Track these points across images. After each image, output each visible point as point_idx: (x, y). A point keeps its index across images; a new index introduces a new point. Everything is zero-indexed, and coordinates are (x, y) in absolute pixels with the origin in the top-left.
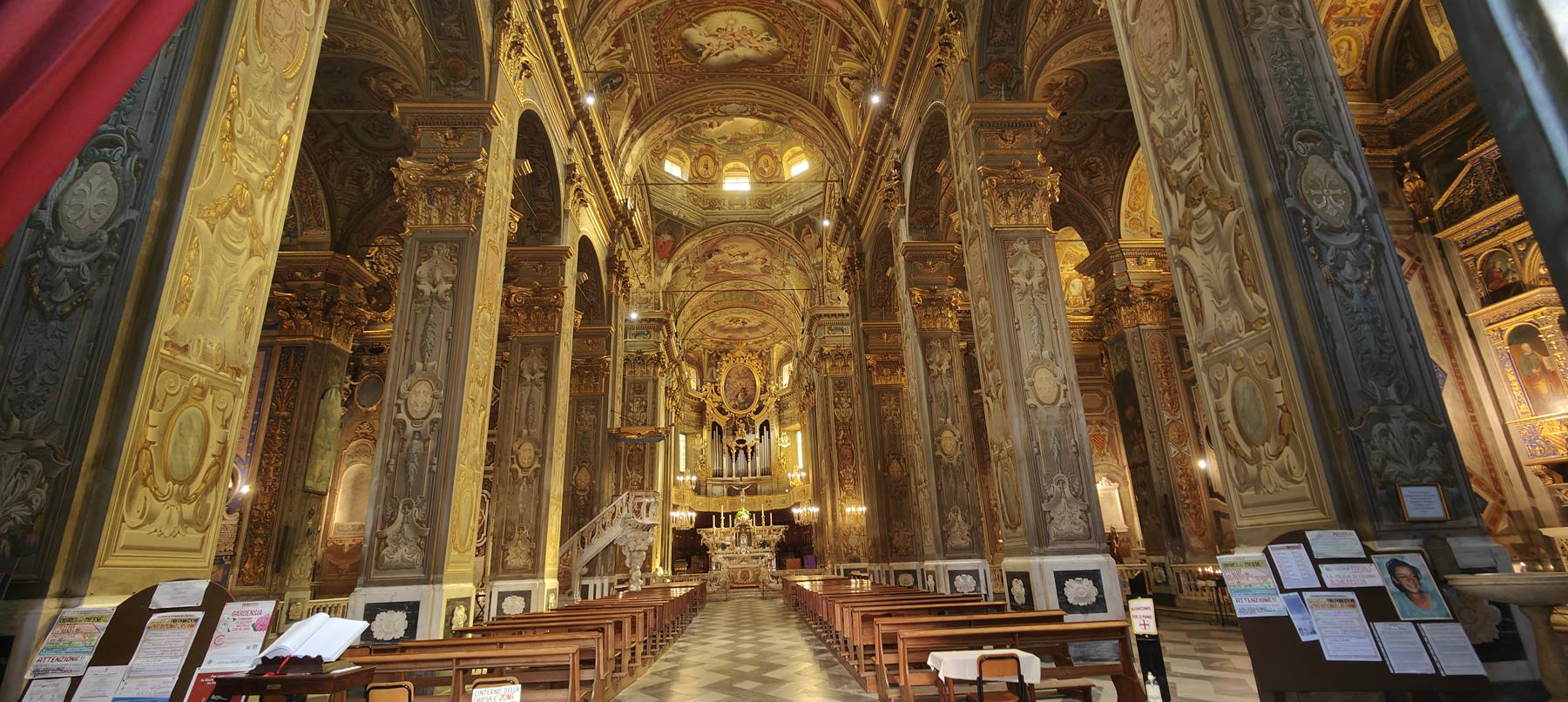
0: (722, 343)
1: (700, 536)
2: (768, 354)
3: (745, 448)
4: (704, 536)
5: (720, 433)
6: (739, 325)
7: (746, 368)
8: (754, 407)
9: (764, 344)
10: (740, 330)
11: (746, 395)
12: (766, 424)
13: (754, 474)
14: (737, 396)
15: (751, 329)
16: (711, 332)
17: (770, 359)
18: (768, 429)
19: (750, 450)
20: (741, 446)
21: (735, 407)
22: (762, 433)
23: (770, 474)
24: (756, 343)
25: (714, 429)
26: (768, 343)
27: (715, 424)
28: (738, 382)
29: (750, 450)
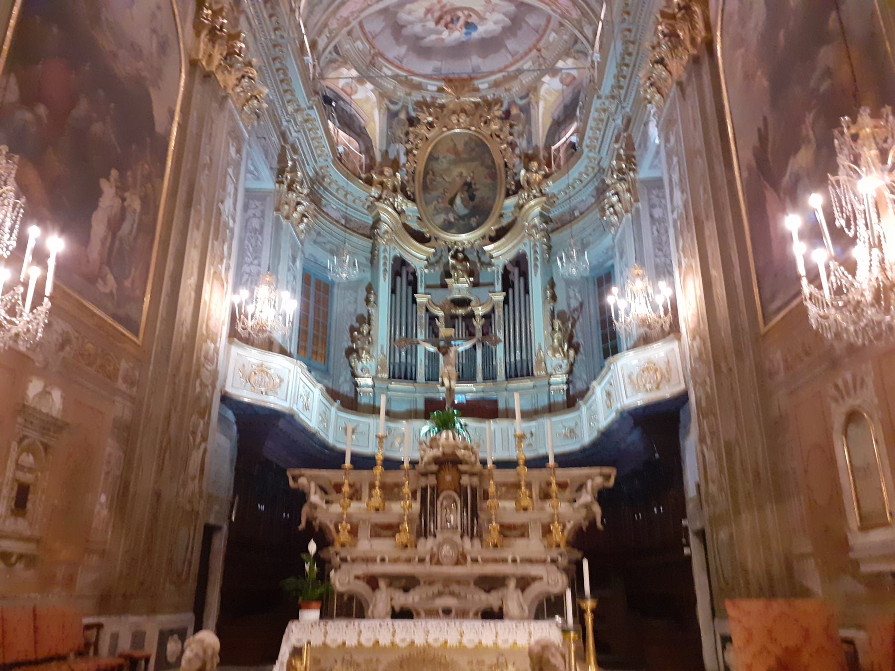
0: (419, 87)
1: (302, 497)
2: (526, 110)
3: (472, 315)
4: (315, 498)
5: (413, 285)
6: (457, 35)
7: (471, 137)
8: (490, 227)
9: (516, 88)
10: (459, 50)
11: (472, 198)
12: (520, 262)
13: (490, 376)
14: (452, 202)
15: (489, 45)
16: (396, 51)
17: (528, 121)
18: (524, 274)
19: (478, 324)
20: (461, 311)
21: (448, 227)
22: (507, 285)
23: (529, 374)
24: (496, 85)
25: (396, 274)
26: (526, 79)
27: (400, 266)
28: (456, 171)
29: (478, 324)
